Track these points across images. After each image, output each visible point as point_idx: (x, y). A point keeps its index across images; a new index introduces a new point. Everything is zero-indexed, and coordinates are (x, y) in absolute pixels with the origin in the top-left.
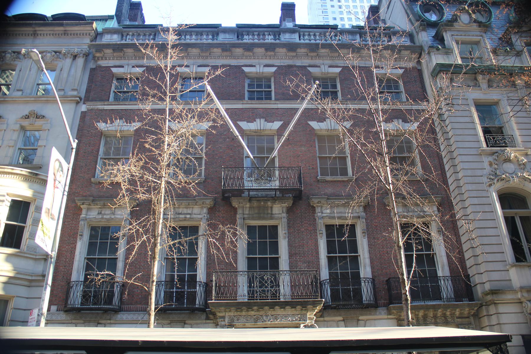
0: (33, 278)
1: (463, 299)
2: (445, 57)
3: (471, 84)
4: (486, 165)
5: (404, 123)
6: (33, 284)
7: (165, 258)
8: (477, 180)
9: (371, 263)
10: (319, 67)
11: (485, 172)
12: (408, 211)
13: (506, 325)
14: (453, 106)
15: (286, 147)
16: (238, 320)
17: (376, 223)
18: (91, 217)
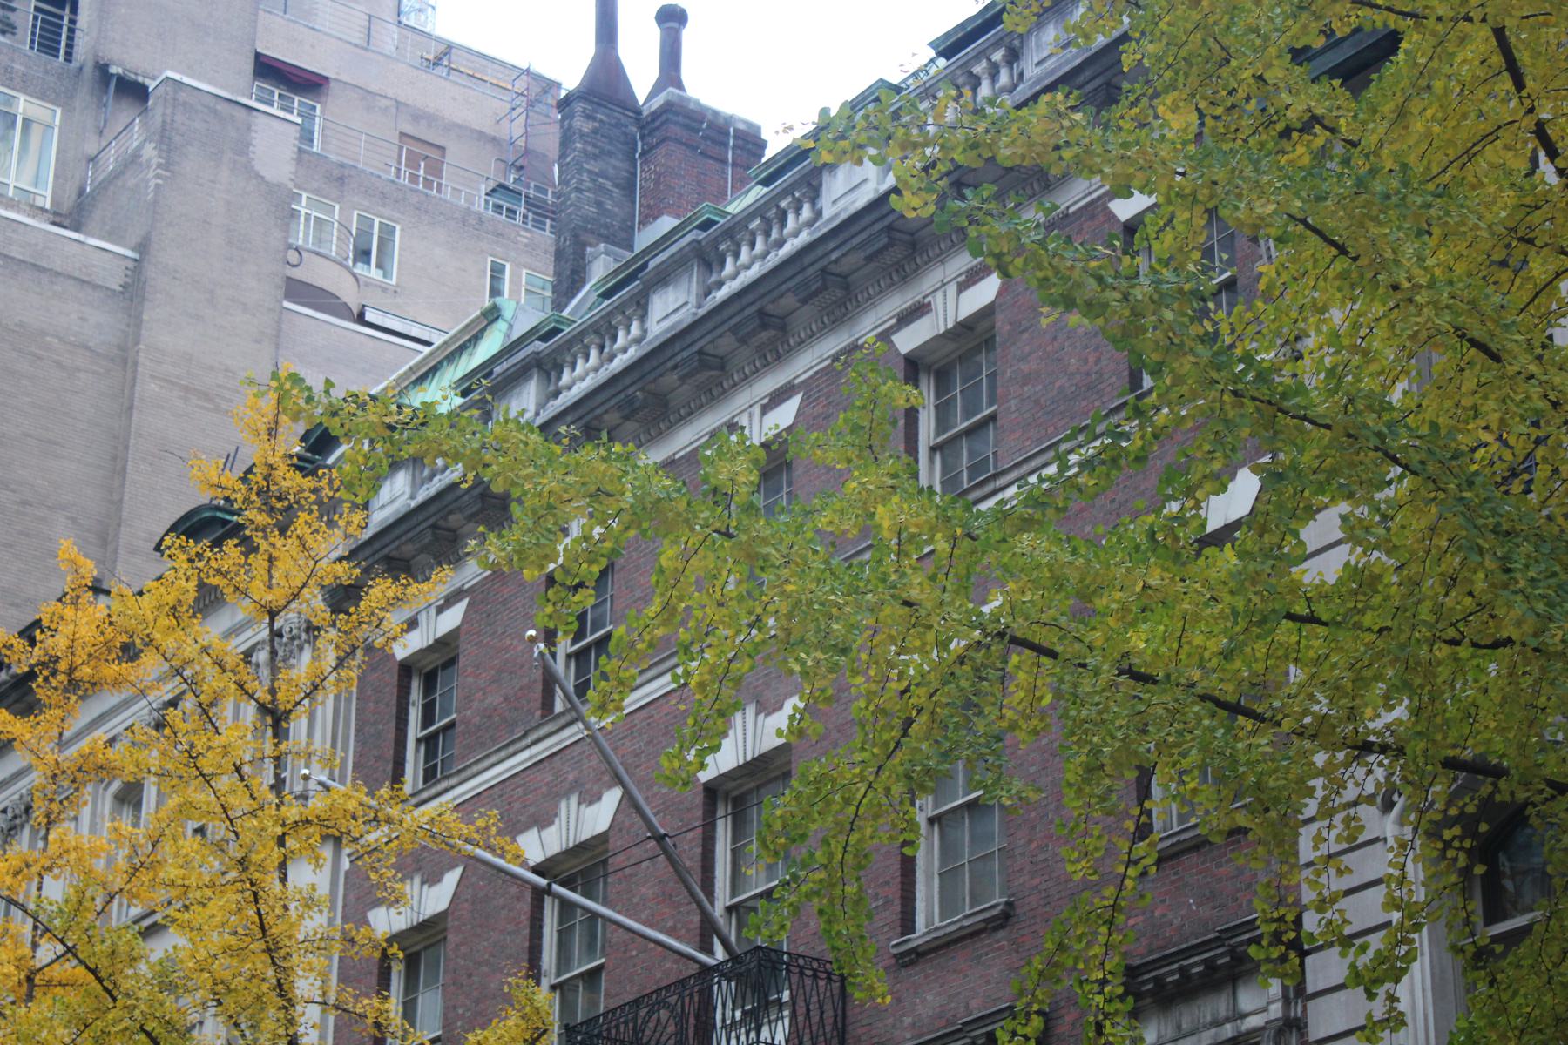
12: (1179, 1027)
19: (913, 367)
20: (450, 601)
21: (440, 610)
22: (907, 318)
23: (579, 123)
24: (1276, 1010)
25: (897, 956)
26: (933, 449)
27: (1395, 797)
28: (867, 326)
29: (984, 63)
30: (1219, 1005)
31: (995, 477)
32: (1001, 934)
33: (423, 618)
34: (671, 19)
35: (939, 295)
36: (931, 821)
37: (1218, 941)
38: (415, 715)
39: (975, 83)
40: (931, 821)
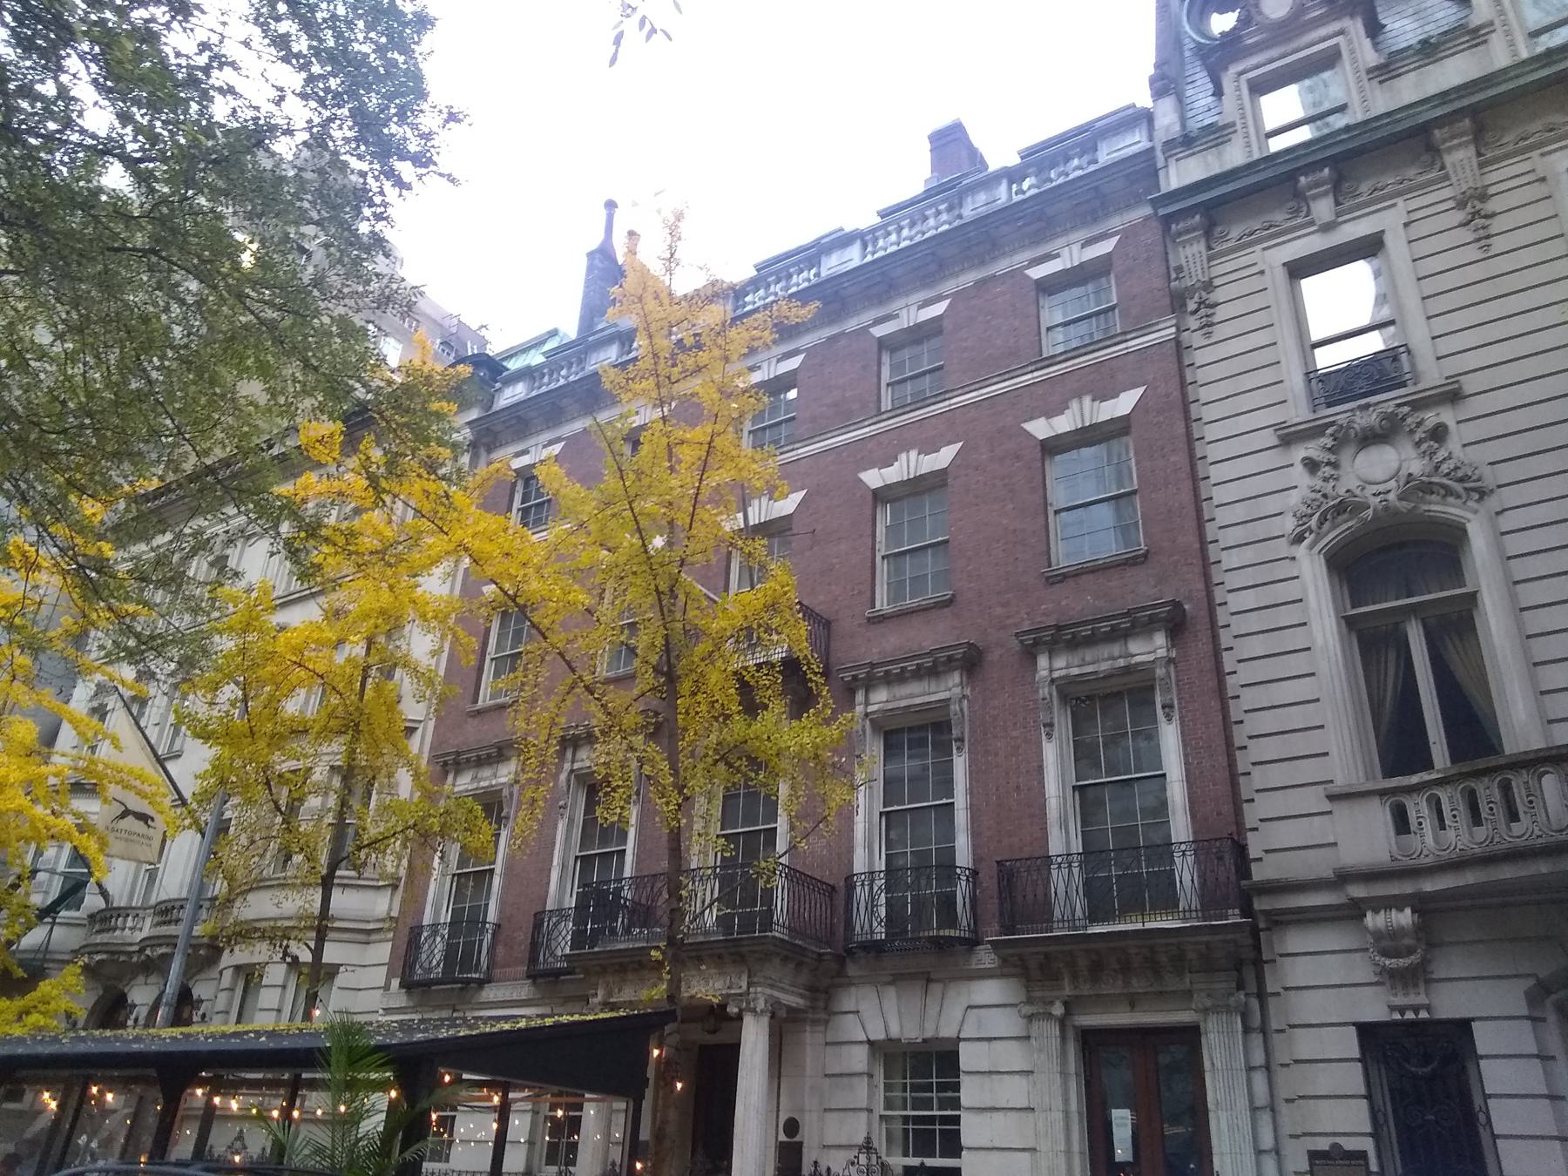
0: (371, 926)
1: (1230, 912)
2: (1210, 157)
3: (1279, 217)
4: (1299, 475)
5: (1097, 403)
6: (374, 937)
7: (577, 857)
8: (1260, 530)
9: (972, 824)
10: (897, 316)
11: (1294, 499)
12: (1083, 660)
13: (1304, 992)
14: (1210, 311)
15: (808, 554)
16: (620, 991)
17: (994, 708)
18: (462, 788)
19: (883, 344)
20: (551, 443)
21: (545, 446)
22: (878, 321)
23: (597, 262)
24: (1162, 653)
25: (869, 619)
26: (888, 385)
27: (1307, 535)
28: (852, 324)
29: (934, 210)
30: (1116, 649)
31: (946, 392)
32: (946, 610)
33: (533, 450)
34: (631, 234)
35: (905, 311)
36: (883, 558)
37: (1128, 614)
38: (518, 498)
39: (926, 218)
40: (883, 558)
